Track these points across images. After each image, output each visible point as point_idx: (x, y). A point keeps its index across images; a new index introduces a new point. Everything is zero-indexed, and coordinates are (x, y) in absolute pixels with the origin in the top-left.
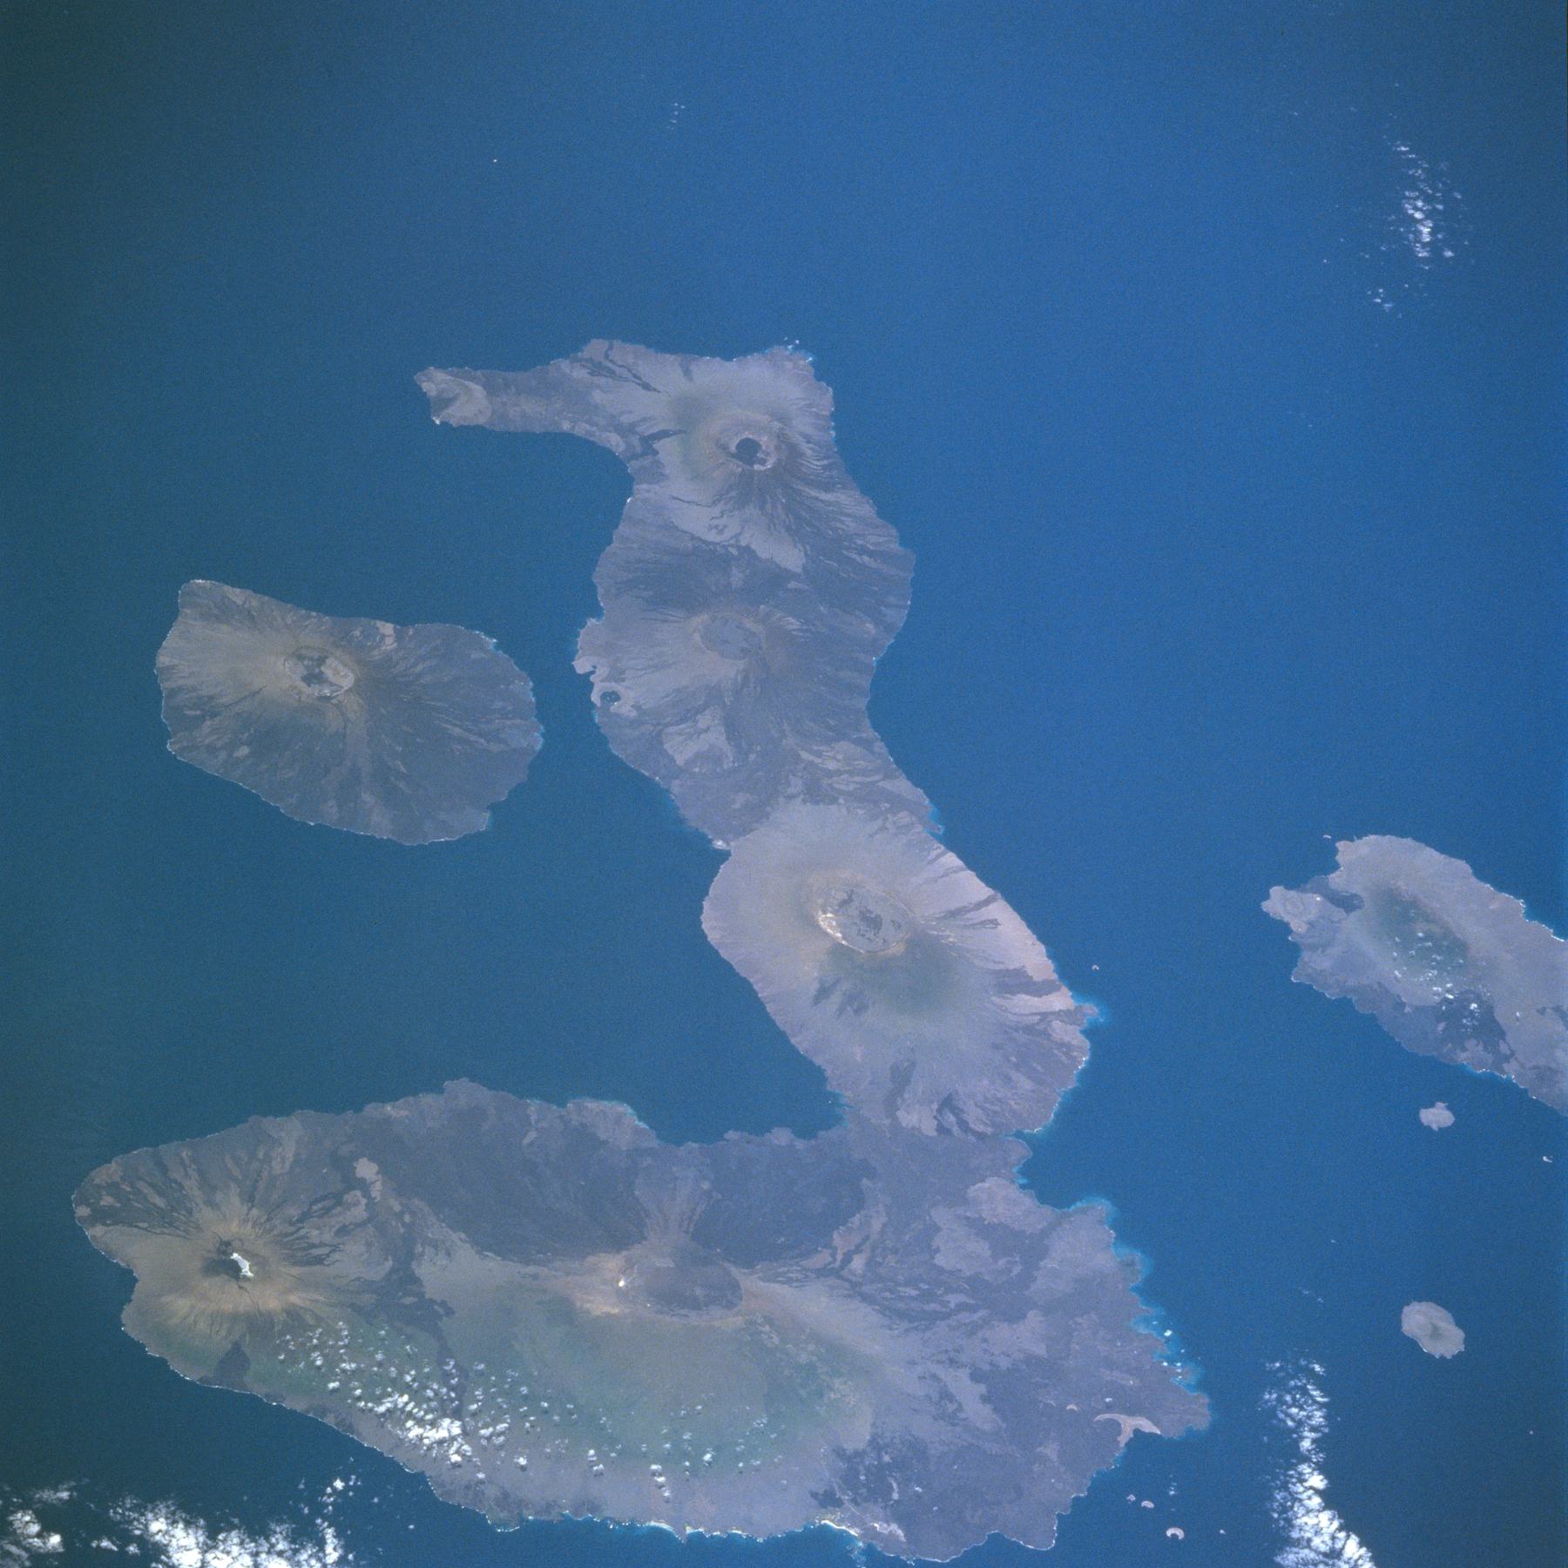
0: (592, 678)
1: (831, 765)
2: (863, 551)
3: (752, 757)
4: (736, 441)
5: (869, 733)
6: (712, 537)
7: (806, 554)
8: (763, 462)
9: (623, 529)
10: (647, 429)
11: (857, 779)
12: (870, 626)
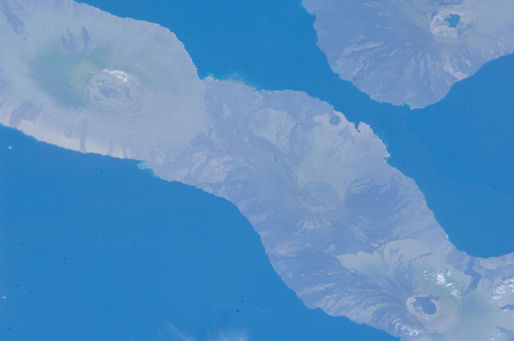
0: (352, 125)
1: (214, 162)
2: (328, 291)
3: (247, 139)
4: (438, 308)
5: (220, 194)
6: (392, 245)
7: (347, 270)
8: (414, 304)
9: (431, 218)
10: (483, 283)
12: (283, 253)
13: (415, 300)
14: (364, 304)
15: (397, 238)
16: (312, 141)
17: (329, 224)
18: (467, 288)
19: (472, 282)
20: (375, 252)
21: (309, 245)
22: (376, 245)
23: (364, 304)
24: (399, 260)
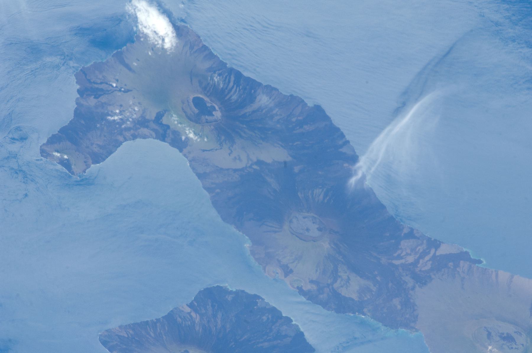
1: (411, 259)
4: (192, 104)
6: (239, 165)
7: (282, 146)
11: (427, 258)
13: (214, 113)
14: (264, 111)
15: (235, 170)
16: (317, 271)
17: (299, 194)
18: (165, 115)
19: (161, 118)
20: (255, 160)
21: (320, 173)
22: (255, 167)
23: (264, 111)
24: (232, 151)
